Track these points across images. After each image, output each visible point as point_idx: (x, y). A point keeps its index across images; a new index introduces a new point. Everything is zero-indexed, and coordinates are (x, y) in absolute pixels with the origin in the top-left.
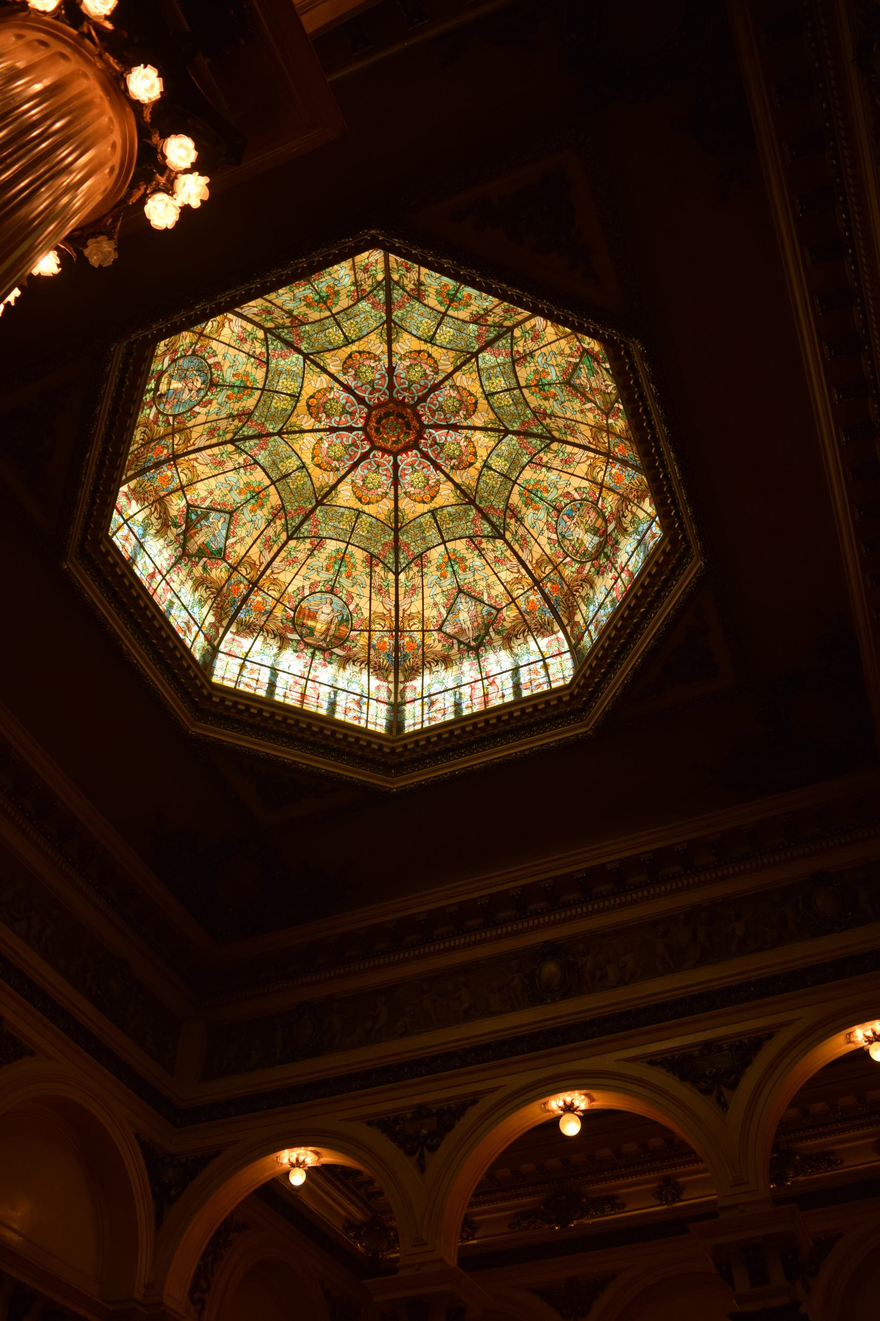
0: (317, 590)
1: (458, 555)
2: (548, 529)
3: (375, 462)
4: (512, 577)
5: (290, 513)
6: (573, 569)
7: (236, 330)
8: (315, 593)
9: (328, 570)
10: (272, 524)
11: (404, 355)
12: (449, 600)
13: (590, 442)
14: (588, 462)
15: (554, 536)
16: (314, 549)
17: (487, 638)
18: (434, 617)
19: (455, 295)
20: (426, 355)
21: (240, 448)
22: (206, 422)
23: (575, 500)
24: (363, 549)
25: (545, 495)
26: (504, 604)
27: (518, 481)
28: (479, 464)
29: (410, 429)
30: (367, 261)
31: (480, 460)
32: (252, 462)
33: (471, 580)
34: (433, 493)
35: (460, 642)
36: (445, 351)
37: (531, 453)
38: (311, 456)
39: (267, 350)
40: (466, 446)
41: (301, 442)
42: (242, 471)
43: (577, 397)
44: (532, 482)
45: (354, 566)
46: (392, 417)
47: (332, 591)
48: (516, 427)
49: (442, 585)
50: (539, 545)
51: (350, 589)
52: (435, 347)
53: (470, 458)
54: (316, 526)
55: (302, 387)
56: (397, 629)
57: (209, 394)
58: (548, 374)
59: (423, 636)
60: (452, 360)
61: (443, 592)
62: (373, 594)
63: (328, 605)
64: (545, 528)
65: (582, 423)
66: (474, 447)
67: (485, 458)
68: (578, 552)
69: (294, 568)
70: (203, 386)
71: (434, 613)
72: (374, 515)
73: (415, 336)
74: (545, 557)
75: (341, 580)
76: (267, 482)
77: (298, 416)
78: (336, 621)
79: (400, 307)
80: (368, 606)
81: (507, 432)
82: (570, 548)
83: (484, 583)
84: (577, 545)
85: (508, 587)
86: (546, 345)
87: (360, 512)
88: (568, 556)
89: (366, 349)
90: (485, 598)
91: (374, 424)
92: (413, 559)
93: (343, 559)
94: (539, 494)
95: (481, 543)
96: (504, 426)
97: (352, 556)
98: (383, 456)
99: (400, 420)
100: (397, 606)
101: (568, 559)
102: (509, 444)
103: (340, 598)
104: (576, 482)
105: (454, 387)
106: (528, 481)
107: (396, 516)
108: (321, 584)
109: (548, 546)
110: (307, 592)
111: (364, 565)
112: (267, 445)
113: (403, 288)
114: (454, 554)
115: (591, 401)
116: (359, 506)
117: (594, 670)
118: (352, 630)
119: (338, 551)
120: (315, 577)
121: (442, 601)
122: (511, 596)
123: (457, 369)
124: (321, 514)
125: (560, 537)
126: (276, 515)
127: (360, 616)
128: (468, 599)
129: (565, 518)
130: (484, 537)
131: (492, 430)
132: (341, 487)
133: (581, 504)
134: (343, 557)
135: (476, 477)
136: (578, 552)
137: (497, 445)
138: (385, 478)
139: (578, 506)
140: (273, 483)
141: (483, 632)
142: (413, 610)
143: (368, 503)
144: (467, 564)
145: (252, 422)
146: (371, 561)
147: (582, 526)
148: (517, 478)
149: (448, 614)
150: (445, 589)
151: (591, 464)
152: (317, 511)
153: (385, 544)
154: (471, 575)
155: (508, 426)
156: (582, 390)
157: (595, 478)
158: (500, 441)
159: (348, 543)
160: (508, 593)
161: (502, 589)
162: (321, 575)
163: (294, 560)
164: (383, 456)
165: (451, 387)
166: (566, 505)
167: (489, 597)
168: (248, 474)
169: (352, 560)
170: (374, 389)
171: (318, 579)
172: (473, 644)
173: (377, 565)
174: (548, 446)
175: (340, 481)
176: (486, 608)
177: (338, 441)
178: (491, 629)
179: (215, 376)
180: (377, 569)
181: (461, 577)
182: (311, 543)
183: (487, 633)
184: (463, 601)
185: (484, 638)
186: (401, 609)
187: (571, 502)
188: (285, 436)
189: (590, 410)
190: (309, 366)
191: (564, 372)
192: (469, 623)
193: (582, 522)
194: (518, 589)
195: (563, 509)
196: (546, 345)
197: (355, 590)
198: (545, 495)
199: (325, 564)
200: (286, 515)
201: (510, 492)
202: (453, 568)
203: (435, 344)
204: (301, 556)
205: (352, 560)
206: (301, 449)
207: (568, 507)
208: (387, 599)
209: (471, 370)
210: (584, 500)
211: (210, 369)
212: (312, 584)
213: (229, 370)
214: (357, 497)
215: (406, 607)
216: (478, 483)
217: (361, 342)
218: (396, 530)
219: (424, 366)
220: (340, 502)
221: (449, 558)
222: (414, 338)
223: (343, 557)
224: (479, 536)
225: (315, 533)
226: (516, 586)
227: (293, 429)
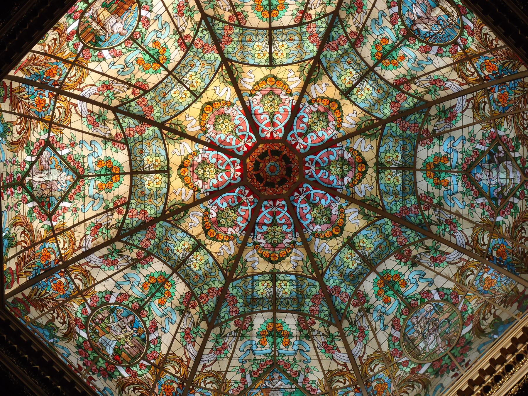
0: (140, 23)
1: (115, 184)
2: (121, 294)
3: (244, 136)
4: (78, 239)
5: (230, 29)
6: (79, 315)
7: (449, 83)
8: (139, 21)
9: (154, 42)
10: (230, 8)
11: (344, 213)
12: (74, 161)
13: (204, 366)
14: (184, 359)
15: (113, 300)
16: (181, 37)
17: (29, 198)
18: (61, 139)
19: (392, 288)
20: (337, 233)
21: (324, 17)
22: (374, 5)
23: (149, 334)
24: (157, 85)
25: (157, 301)
26: (54, 224)
27: (175, 275)
28: (202, 237)
29: (264, 186)
30: (459, 229)
31: (207, 241)
32: (304, 21)
33: (86, 193)
34: (187, 180)
35: (32, 164)
36: (334, 252)
37: (202, 298)
38: (279, 76)
39: (410, 95)
40: (226, 233)
41: (298, 74)
42: (303, 8)
43: (258, 370)
44: (172, 290)
45: (145, 69)
46: (285, 173)
47: (132, 38)
48: (232, 291)
49: (90, 158)
50: (105, 279)
51: (123, 57)
52: (341, 245)
53: (212, 232)
54: (203, 47)
55: (354, 103)
56: (60, 92)
57: (402, 27)
58: (287, 346)
59: (46, 122)
60: (322, 254)
61: (83, 157)
62: (106, 78)
63: (121, 30)
64: (122, 291)
65: (228, 366)
66: (223, 241)
67: (208, 247)
68: (97, 324)
69: (174, 9)
70: (415, 28)
71: (66, 141)
72: (187, 111)
73: (360, 231)
74: (92, 283)
75: (138, 51)
76: (275, 24)
77: (326, 85)
78: (101, 33)
79: (395, 231)
80: (98, 69)
81: (229, 279)
82: (100, 316)
83: (79, 205)
84: (104, 326)
85: (69, 232)
86: (318, 356)
87: (197, 98)
88: (93, 311)
89: (364, 181)
90: (66, 204)
91: (285, 152)
92: (124, 133)
93: (157, 61)
94: (158, 294)
95: (119, 213)
96: (236, 279)
97: (156, 71)
98: (247, 146)
99: (278, 180)
100: (82, 99)
101: (89, 311)
102: (216, 277)
103: (120, 44)
104: (166, 339)
105: (293, 244)
106: (173, 285)
107: (176, 132)
108: (143, 30)
109: (103, 290)
110: (144, 13)
111: (141, 80)
112: (312, 42)
113: (414, 243)
114: (117, 180)
115: (254, 382)
116: (205, 99)
117: (27, 345)
118: (85, 45)
119: (168, 59)
120: (154, 26)
121: (75, 153)
122: (59, 234)
123: (311, 256)
124: (212, 58)
125: (112, 306)
126: (237, 16)
127: (93, 58)
128: (69, 183)
129: (131, 318)
130: (124, 218)
131: (235, 265)
132: (231, 90)
133: (144, 340)
134: (158, 62)
135: (190, 231)
136: (97, 324)
137: (218, 264)
138: (223, 138)
139: (143, 336)
140: (271, 29)
141: (35, 193)
142: (74, 117)
143: (203, 110)
144: (103, 192)
145: (344, 41)
146: (140, 89)
147: (122, 336)
148: (179, 275)
149: (61, 157)
150: (85, 160)
151: (182, 361)
152: (217, 55)
153: (151, 109)
154: (91, 193)
155: (235, 283)
156: (267, 377)
157: (169, 362)
158: (221, 269)
159: (170, 73)
160: (64, 231)
161: (69, 224)
162: (153, 33)
163: (180, 12)
164: (247, 146)
165: (294, 243)
166: (144, 322)
167: (66, 209)
168: (295, 12)
169: (151, 70)
170: (321, 168)
171: (150, 29)
172: (27, 179)
173: (134, 93)
174: (205, 318)
175: (239, 92)
176: (55, 203)
177: (281, 110)
178: (35, 204)
179: (417, 42)
180: (129, 92)
181: (92, 181)
182: (188, 36)
183: (33, 199)
184: (69, 177)
185: (31, 194)
186: (78, 102)
187: (147, 329)
188: (311, 63)
189: (244, 379)
190: (372, 120)
191: (287, 364)
192: (47, 179)
193: (126, 337)
194: (65, 242)
195: (141, 317)
196: (318, 356)
197: (120, 62)
198: (157, 301)
199: (162, 42)
200: (230, 24)
201: (165, 263)
202: (104, 175)
203: (344, 246)
204: (180, 21)
205: (151, 70)
206: (291, 71)
207: (141, 323)
208: (94, 90)
209: (305, 269)
210: (148, 345)
211: (427, 43)
212: (148, 21)
213: (413, 56)
214: (214, 101)
215: (79, 109)
216: (183, 231)
217: (374, 179)
218: (161, 126)
219: (326, 225)
220: (216, 82)
221: (115, 174)
222: (358, 229)
223: (158, 62)
224: (126, 213)
225: (197, 44)
226: (67, 240)
227: (315, 73)
